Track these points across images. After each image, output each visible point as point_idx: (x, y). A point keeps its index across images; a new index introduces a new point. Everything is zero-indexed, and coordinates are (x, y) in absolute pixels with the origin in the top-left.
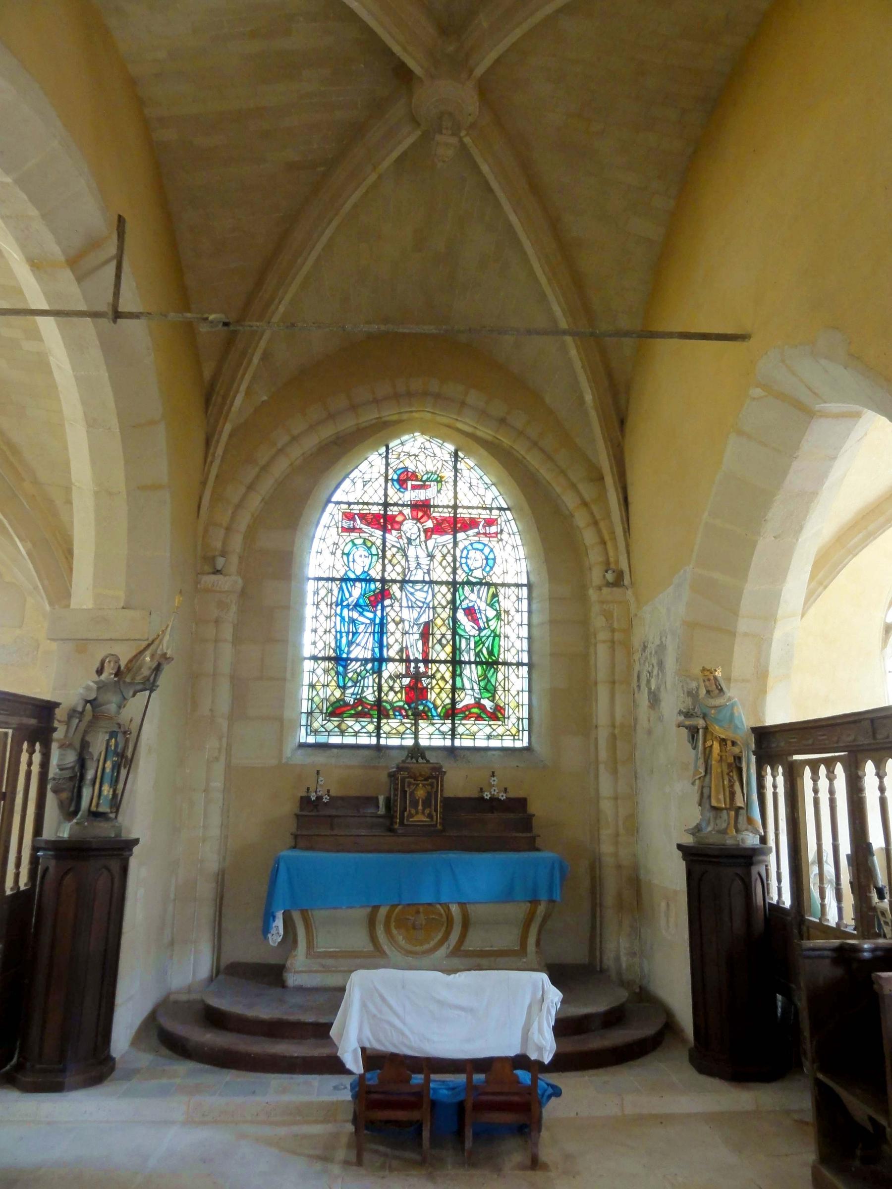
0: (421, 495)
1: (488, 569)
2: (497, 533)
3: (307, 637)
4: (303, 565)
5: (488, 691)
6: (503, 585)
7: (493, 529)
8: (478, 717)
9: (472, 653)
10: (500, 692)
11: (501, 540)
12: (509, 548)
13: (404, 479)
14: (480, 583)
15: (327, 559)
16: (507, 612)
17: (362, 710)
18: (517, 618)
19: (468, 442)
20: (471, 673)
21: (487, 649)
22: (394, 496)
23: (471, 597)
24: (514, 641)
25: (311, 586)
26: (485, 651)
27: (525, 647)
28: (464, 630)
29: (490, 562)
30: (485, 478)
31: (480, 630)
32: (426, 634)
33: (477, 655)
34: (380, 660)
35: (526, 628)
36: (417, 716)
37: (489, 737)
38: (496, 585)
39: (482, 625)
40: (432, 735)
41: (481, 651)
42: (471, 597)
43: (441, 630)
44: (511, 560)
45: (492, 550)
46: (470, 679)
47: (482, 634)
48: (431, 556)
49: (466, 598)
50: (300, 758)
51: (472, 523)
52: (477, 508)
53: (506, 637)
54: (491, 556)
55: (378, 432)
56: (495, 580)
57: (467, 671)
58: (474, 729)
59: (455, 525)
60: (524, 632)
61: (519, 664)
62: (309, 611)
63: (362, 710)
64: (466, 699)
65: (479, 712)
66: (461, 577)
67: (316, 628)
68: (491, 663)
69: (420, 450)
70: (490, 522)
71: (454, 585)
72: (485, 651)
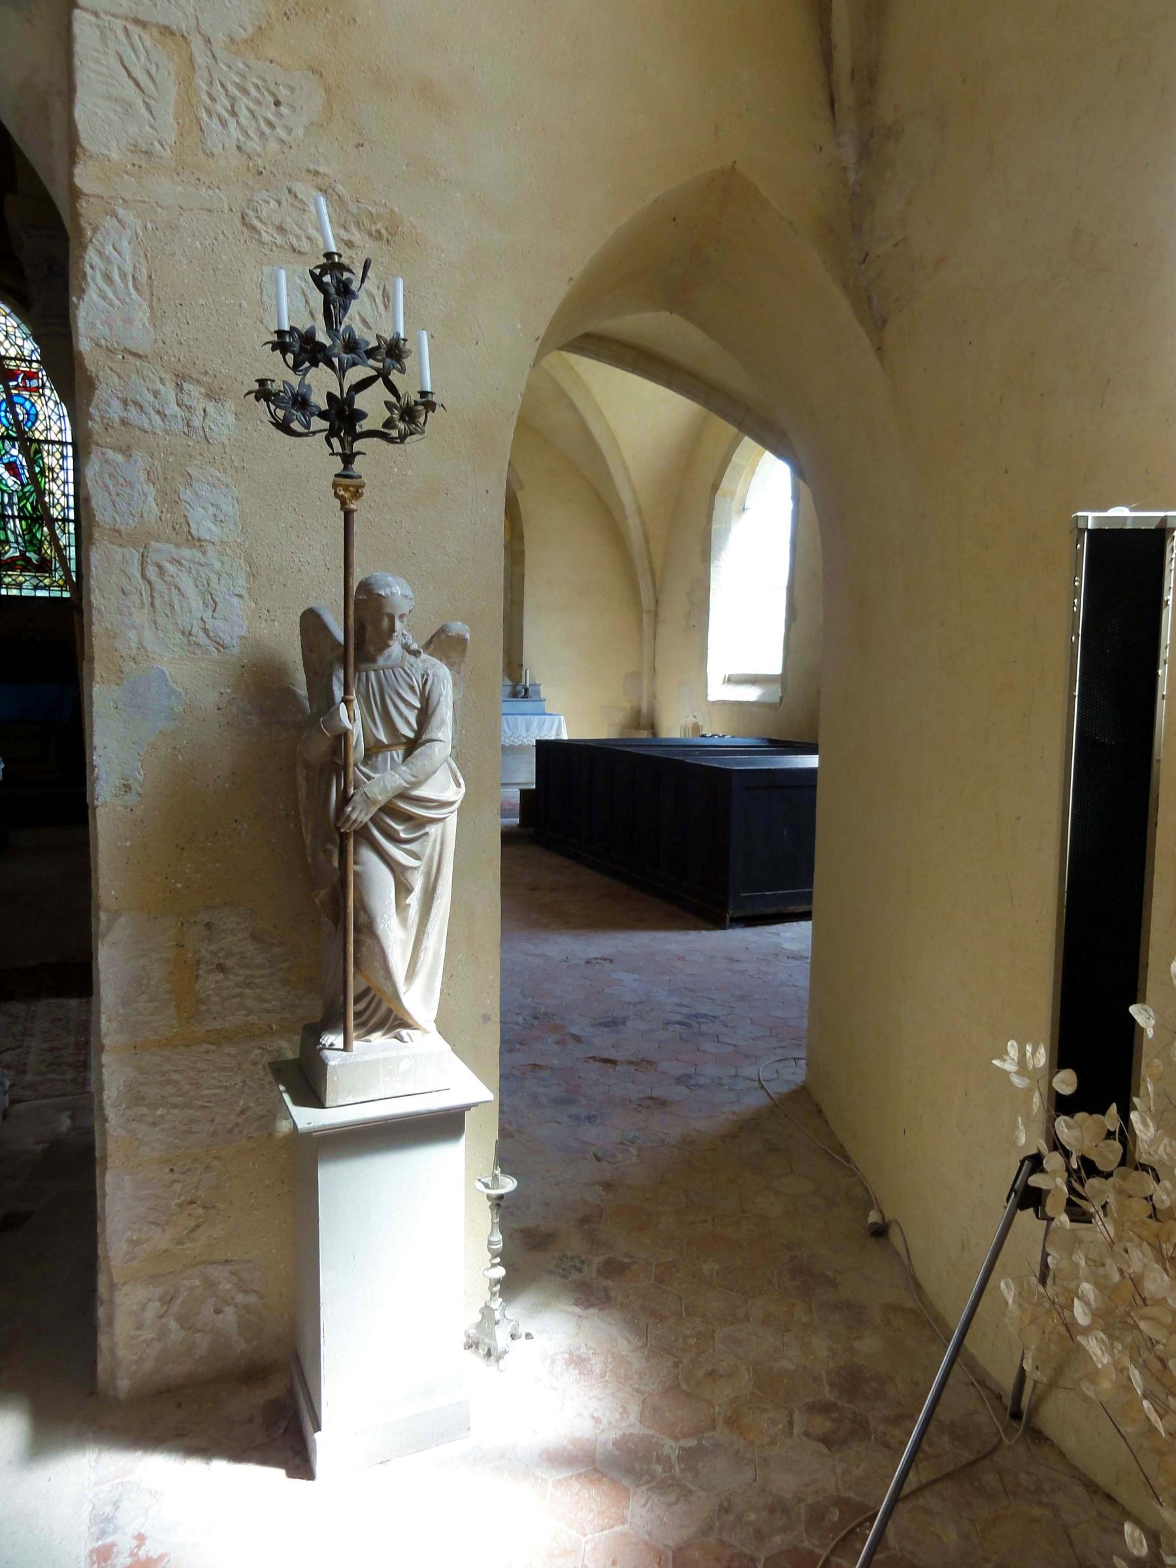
1: (29, 424)
2: (38, 388)
5: (34, 545)
6: (47, 441)
7: (34, 383)
8: (24, 569)
9: (15, 508)
10: (45, 547)
11: (43, 395)
12: (51, 404)
16: (51, 469)
18: (62, 475)
21: (32, 504)
26: (29, 506)
27: (72, 504)
28: (6, 485)
30: (23, 326)
31: (23, 485)
33: (20, 510)
35: (71, 486)
37: (36, 588)
38: (39, 441)
39: (25, 481)
41: (25, 505)
44: (55, 417)
45: (33, 405)
46: (14, 532)
47: (26, 489)
49: (7, 453)
52: (15, 359)
53: (51, 493)
54: (33, 411)
56: (37, 435)
57: (11, 525)
58: (21, 579)
60: (71, 489)
61: (65, 520)
70: (30, 376)
72: (29, 506)
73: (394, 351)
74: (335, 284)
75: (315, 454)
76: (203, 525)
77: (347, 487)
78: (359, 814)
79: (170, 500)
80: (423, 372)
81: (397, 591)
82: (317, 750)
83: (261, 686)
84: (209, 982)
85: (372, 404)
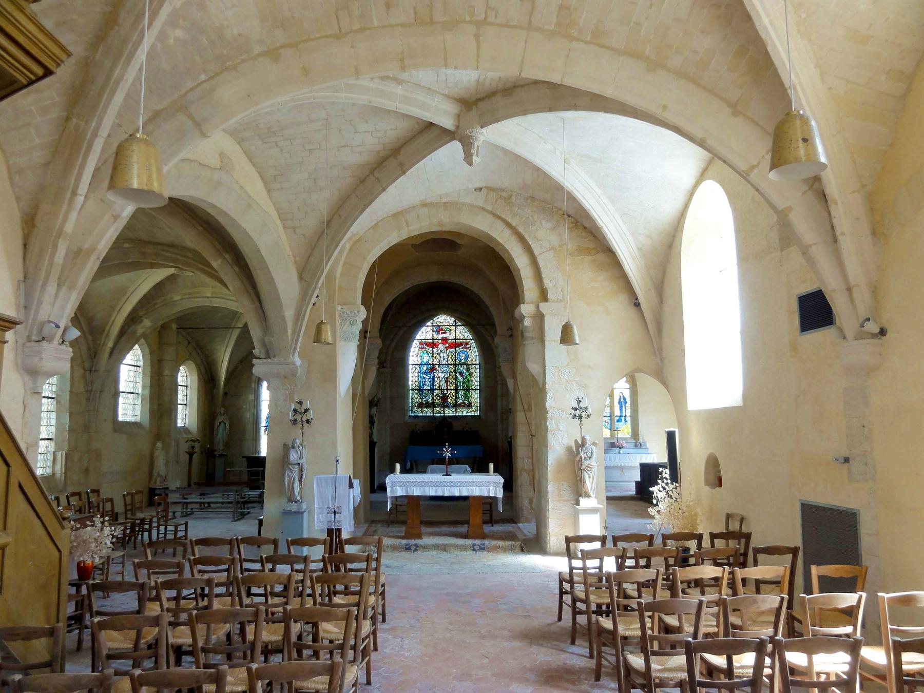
0: (444, 336)
3: (410, 383)
4: (408, 360)
13: (439, 329)
14: (464, 364)
15: (415, 358)
17: (428, 405)
19: (457, 318)
20: (461, 393)
22: (436, 336)
23: (462, 369)
24: (475, 382)
25: (411, 367)
29: (467, 357)
32: (447, 381)
34: (432, 390)
36: (444, 407)
40: (448, 413)
42: (462, 369)
43: (452, 380)
48: (448, 356)
50: (410, 420)
51: (461, 344)
55: (431, 317)
59: (455, 345)
62: (410, 375)
63: (428, 405)
64: (460, 401)
65: (463, 405)
66: (458, 362)
67: (412, 379)
68: (468, 390)
69: (444, 319)
70: (467, 344)
71: (455, 365)
73: (586, 408)
74: (579, 402)
75: (577, 421)
76: (561, 428)
77: (581, 424)
78: (583, 467)
79: (557, 425)
80: (590, 411)
81: (588, 437)
82: (578, 459)
83: (569, 449)
84: (562, 492)
85: (584, 415)
